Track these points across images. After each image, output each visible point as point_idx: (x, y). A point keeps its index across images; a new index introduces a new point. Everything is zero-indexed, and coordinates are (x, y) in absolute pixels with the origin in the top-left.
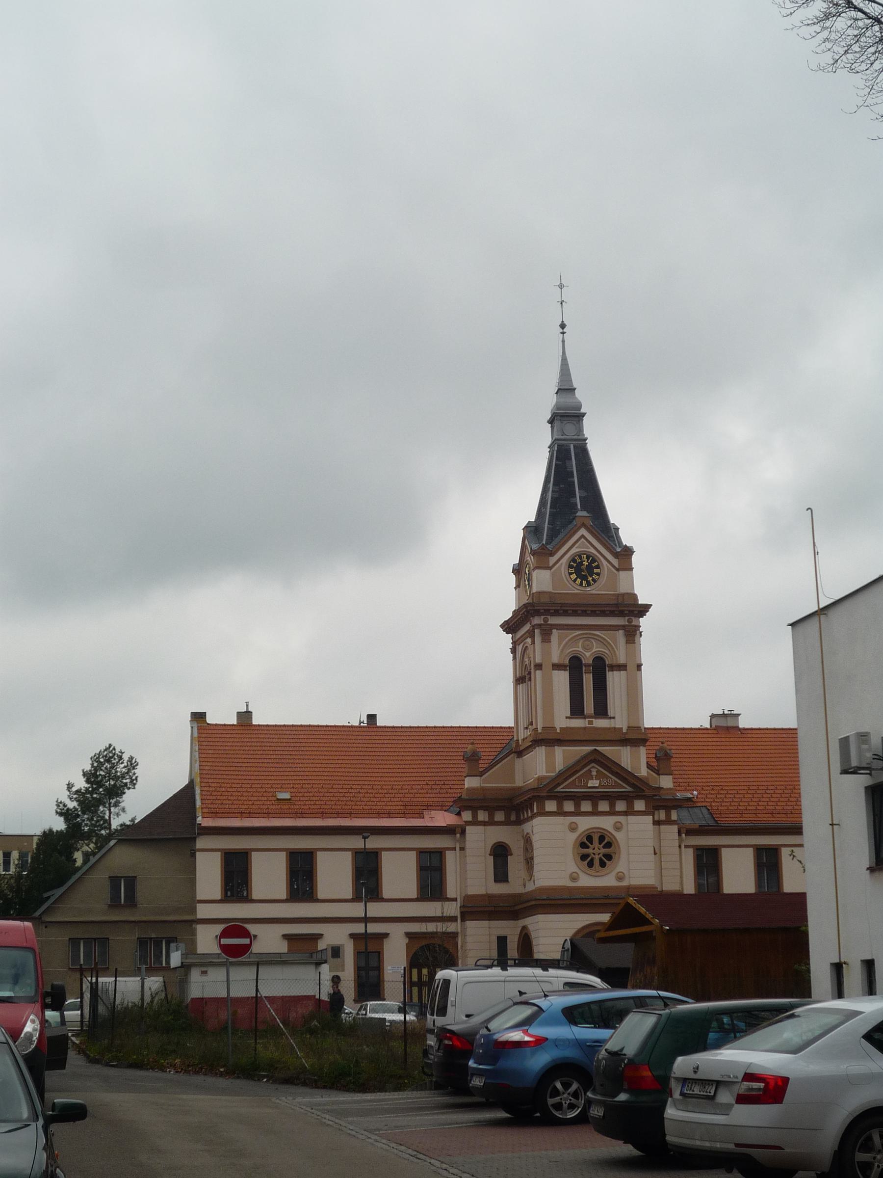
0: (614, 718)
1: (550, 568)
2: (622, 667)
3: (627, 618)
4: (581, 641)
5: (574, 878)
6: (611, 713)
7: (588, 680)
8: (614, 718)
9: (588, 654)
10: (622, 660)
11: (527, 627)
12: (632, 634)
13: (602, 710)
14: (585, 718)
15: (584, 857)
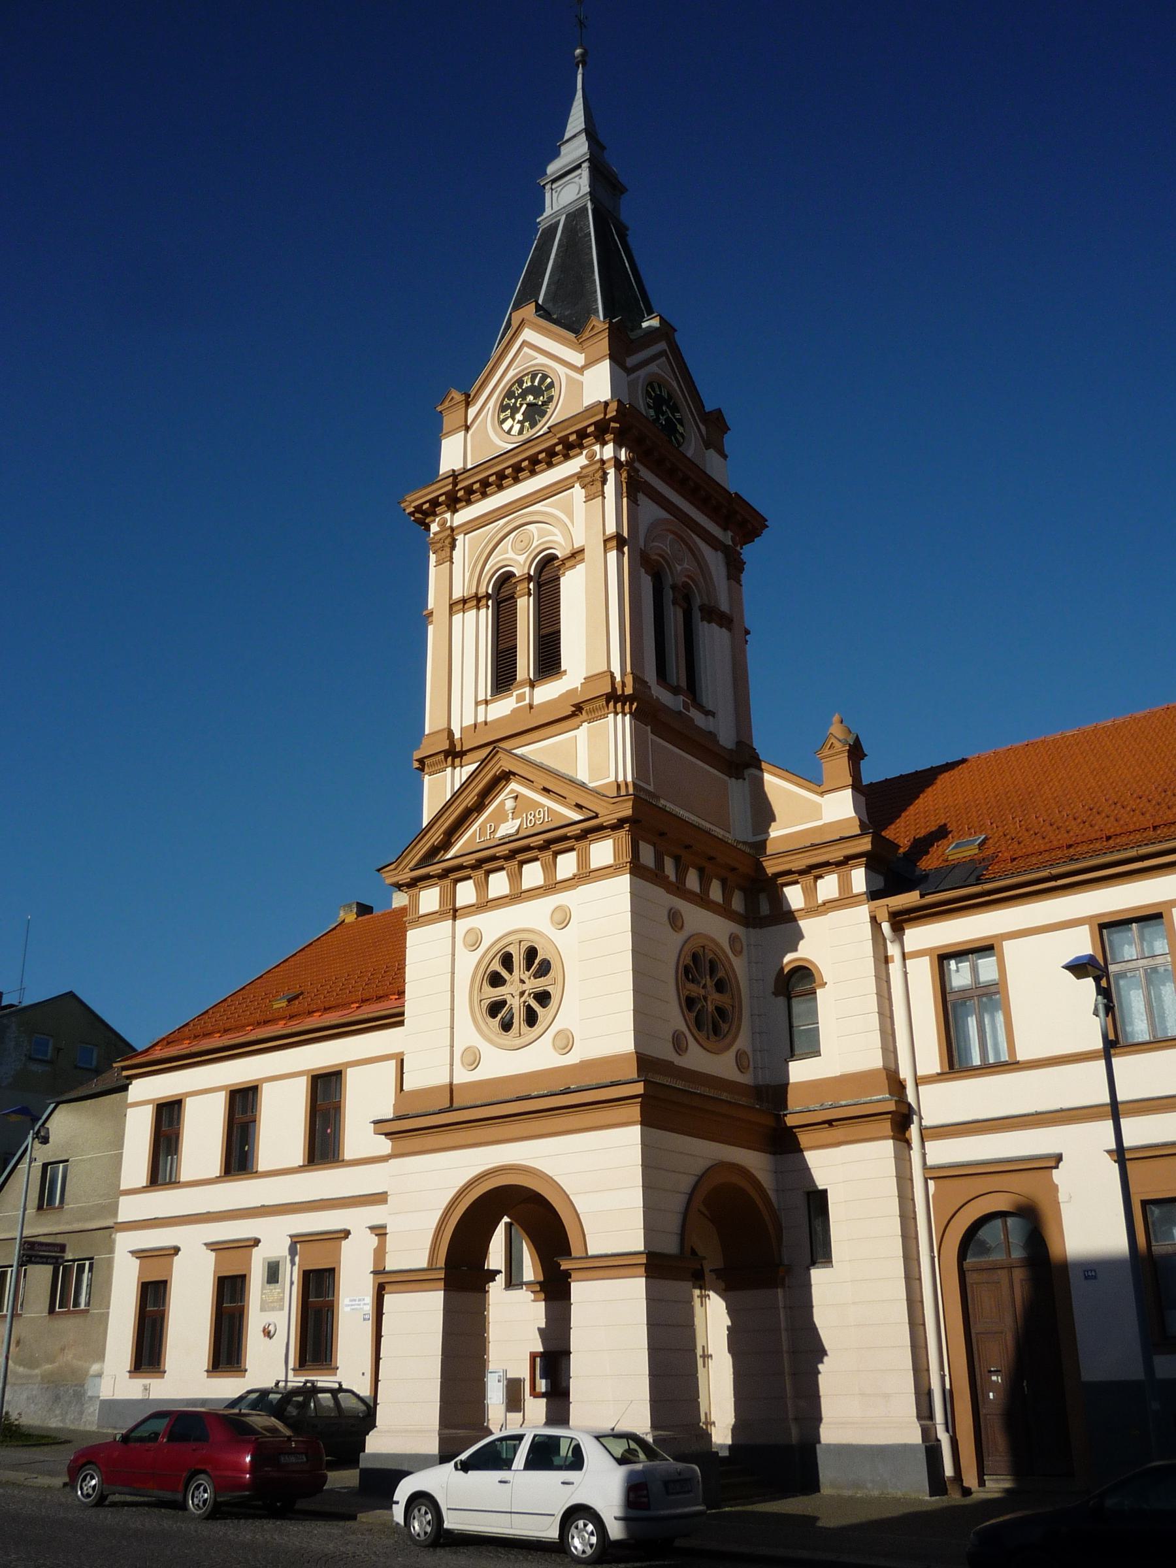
0: (713, 714)
1: (629, 371)
2: (726, 621)
3: (730, 534)
4: (671, 536)
5: (678, 1044)
6: (709, 702)
7: (674, 616)
8: (713, 714)
9: (679, 568)
10: (724, 606)
11: (577, 464)
12: (735, 567)
13: (692, 689)
14: (675, 691)
15: (689, 1003)
